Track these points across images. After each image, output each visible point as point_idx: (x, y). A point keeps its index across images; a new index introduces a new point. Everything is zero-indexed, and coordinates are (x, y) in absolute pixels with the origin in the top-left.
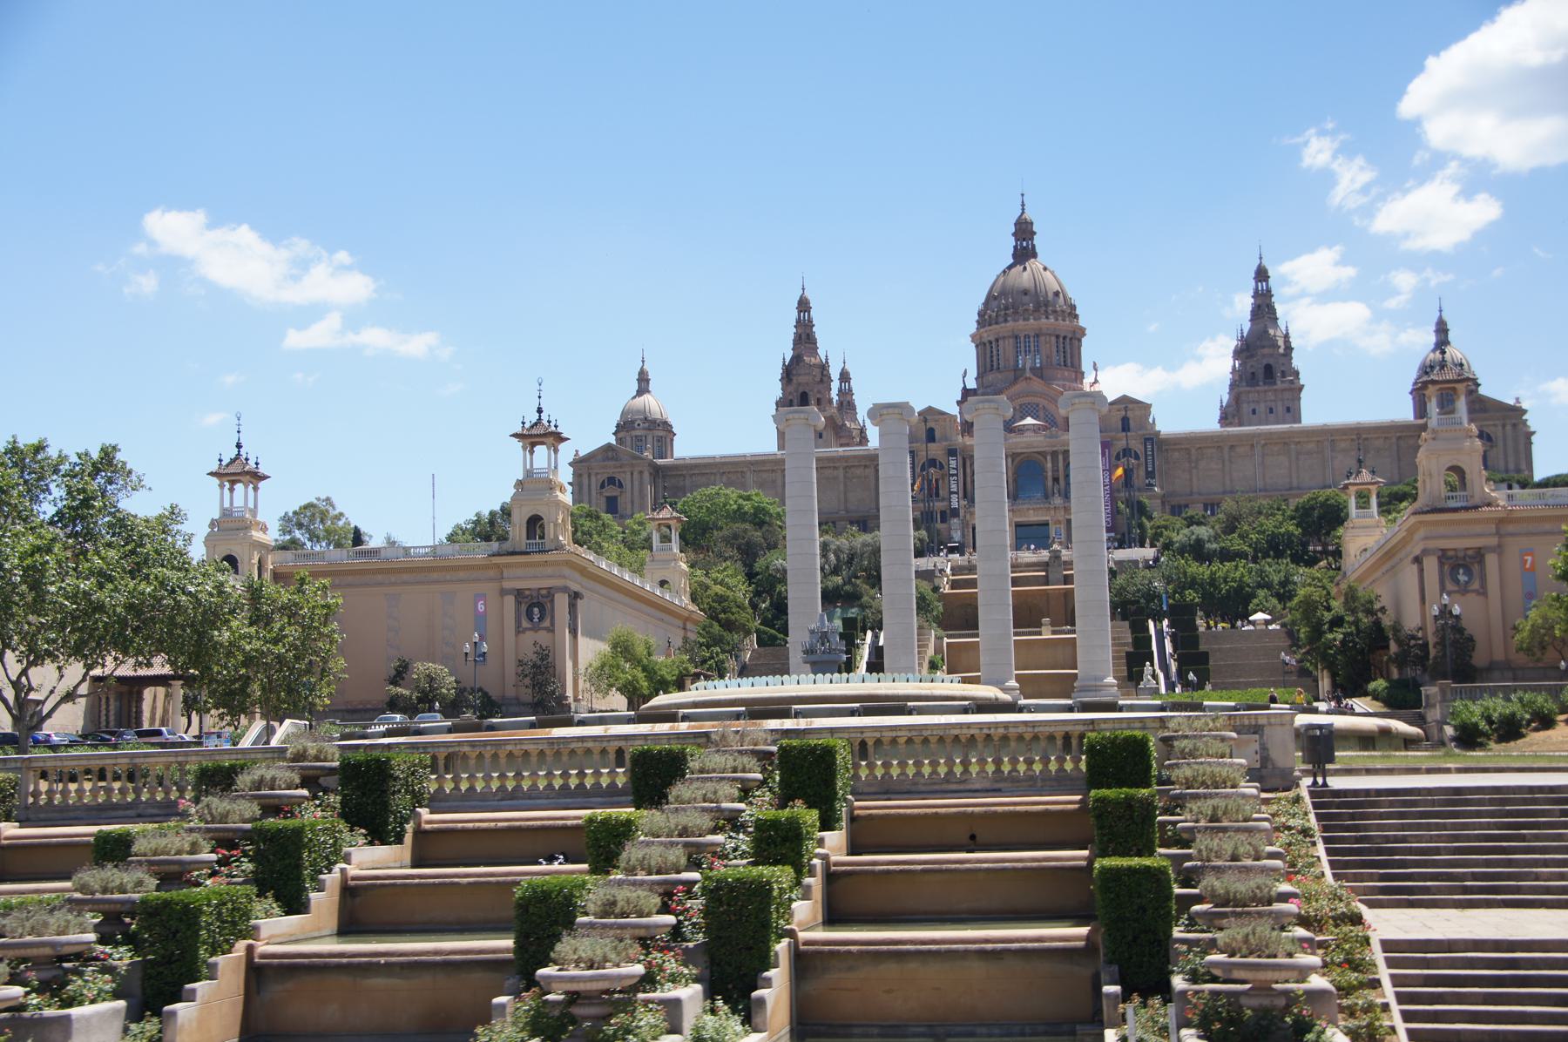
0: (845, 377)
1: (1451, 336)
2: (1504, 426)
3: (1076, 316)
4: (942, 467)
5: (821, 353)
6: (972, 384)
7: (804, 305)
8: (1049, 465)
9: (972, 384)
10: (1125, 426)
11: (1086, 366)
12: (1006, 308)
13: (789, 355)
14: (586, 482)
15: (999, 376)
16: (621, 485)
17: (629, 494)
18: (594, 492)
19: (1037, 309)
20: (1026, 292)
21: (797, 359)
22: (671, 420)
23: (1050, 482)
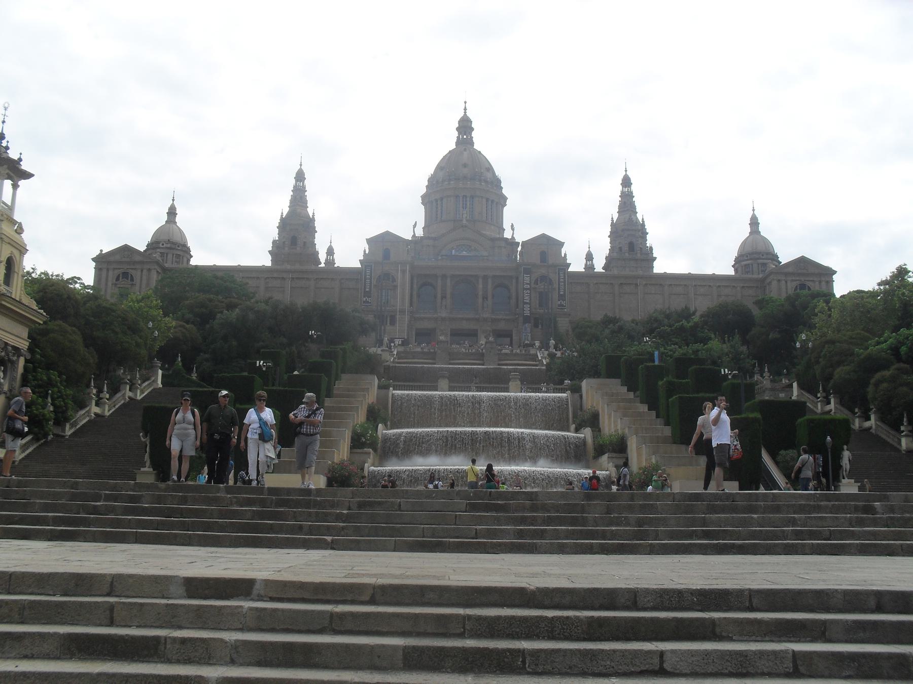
0: (330, 252)
1: (761, 228)
4: (394, 280)
5: (310, 211)
6: (420, 232)
7: (300, 176)
8: (481, 286)
9: (420, 232)
13: (286, 210)
14: (104, 273)
16: (132, 280)
17: (137, 288)
18: (110, 284)
20: (465, 165)
22: (190, 244)
23: (480, 300)
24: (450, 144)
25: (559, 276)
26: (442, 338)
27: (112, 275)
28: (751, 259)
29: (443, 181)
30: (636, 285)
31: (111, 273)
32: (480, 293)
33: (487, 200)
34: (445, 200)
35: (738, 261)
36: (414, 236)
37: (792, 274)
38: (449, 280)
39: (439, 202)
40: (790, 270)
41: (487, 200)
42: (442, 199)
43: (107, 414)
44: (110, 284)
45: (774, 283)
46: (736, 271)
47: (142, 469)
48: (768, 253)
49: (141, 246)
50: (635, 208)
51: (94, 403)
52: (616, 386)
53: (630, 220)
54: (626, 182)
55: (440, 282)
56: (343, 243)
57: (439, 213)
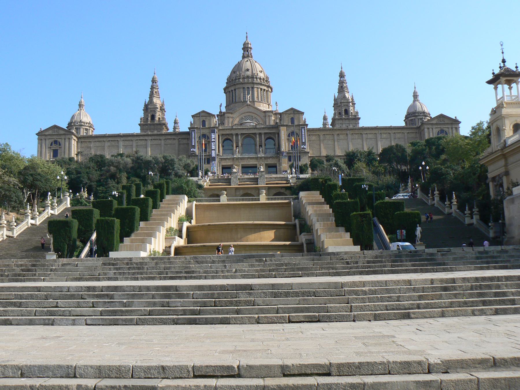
1: (419, 98)
2: (452, 128)
4: (208, 138)
6: (224, 110)
8: (258, 139)
9: (224, 110)
10: (292, 120)
11: (273, 103)
13: (148, 100)
14: (44, 141)
15: (236, 105)
16: (60, 145)
18: (47, 147)
19: (253, 78)
20: (248, 70)
23: (258, 147)
25: (302, 132)
26: (235, 170)
27: (48, 142)
28: (414, 116)
29: (236, 79)
31: (47, 141)
32: (258, 143)
33: (261, 89)
34: (237, 90)
35: (407, 117)
36: (221, 112)
37: (436, 124)
38: (240, 136)
39: (234, 92)
40: (434, 122)
41: (261, 89)
42: (235, 90)
43: (38, 223)
44: (47, 147)
45: (426, 130)
46: (406, 123)
47: (49, 253)
48: (424, 112)
49: (64, 126)
51: (30, 217)
52: (316, 195)
53: (345, 97)
54: (342, 75)
55: (234, 137)
56: (178, 116)
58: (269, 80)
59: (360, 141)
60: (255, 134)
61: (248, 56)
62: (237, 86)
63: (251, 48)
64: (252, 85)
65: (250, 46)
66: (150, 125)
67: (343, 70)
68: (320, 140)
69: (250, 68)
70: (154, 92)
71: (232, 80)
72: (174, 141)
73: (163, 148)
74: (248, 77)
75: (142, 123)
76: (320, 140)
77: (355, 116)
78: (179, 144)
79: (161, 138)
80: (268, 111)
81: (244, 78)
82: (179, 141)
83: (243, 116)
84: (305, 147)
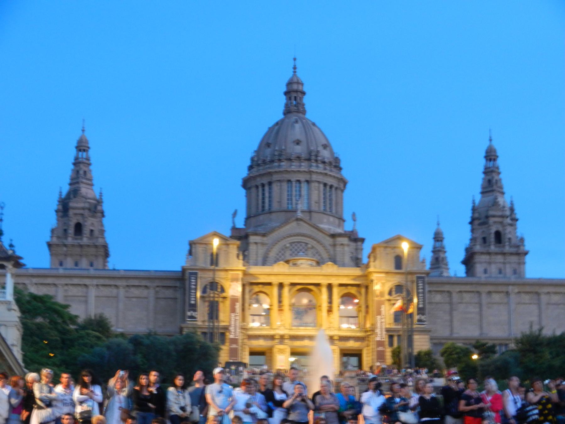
3: (340, 169)
6: (240, 223)
9: (240, 223)
11: (347, 216)
12: (280, 155)
20: (298, 143)
21: (74, 192)
24: (276, 112)
30: (507, 293)
33: (325, 185)
36: (234, 229)
39: (267, 188)
41: (325, 185)
42: (270, 183)
50: (501, 187)
53: (495, 203)
54: (491, 155)
57: (267, 200)
58: (342, 165)
59: (534, 308)
60: (318, 285)
61: (298, 112)
62: (275, 177)
63: (304, 93)
64: (307, 177)
65: (300, 88)
66: (73, 246)
67: (496, 145)
68: (451, 303)
69: (302, 137)
70: (81, 172)
71: (264, 162)
72: (145, 292)
73: (121, 306)
74: (299, 158)
75: (55, 240)
76: (451, 303)
77: (518, 247)
78: (157, 298)
79: (119, 283)
80: (340, 235)
81: (290, 160)
82: (157, 292)
83: (286, 242)
84: (423, 318)
